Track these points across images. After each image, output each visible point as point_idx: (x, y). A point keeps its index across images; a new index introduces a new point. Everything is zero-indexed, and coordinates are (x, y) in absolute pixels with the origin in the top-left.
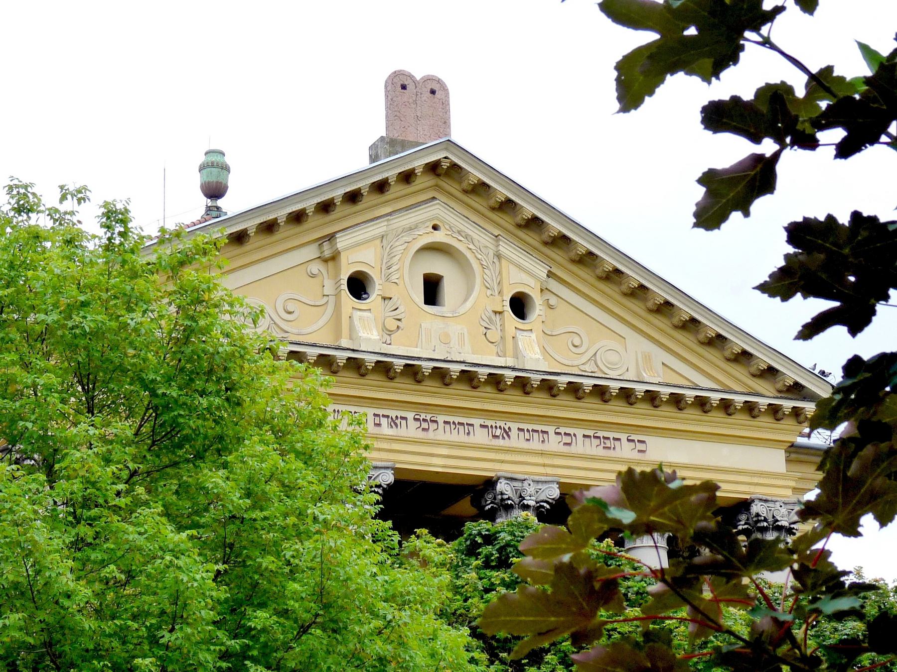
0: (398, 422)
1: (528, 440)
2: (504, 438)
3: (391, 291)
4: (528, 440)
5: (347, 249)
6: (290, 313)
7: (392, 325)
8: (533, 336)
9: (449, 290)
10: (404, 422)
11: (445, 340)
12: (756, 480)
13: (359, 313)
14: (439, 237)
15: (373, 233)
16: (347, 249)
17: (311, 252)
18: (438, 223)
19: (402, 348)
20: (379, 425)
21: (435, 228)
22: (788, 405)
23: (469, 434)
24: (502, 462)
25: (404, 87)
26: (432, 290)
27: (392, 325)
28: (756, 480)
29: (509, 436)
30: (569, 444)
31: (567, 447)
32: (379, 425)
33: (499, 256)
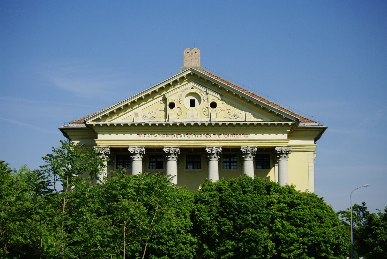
0: (182, 136)
1: (216, 137)
2: (209, 137)
3: (180, 105)
4: (216, 137)
5: (169, 97)
6: (155, 113)
7: (180, 113)
8: (216, 112)
9: (197, 102)
10: (184, 136)
11: (192, 116)
12: (277, 141)
13: (171, 112)
14: (193, 91)
15: (175, 92)
16: (169, 97)
17: (161, 98)
18: (192, 87)
19: (185, 119)
20: (178, 137)
21: (192, 88)
22: (283, 123)
23: (200, 137)
24: (208, 143)
25: (188, 53)
26: (192, 103)
27: (180, 113)
28: (277, 141)
29: (211, 137)
30: (227, 137)
31: (226, 138)
32: (178, 137)
33: (207, 94)
